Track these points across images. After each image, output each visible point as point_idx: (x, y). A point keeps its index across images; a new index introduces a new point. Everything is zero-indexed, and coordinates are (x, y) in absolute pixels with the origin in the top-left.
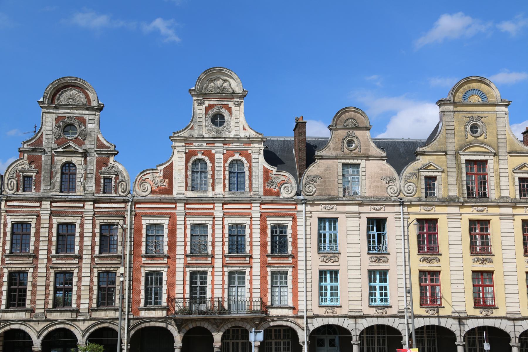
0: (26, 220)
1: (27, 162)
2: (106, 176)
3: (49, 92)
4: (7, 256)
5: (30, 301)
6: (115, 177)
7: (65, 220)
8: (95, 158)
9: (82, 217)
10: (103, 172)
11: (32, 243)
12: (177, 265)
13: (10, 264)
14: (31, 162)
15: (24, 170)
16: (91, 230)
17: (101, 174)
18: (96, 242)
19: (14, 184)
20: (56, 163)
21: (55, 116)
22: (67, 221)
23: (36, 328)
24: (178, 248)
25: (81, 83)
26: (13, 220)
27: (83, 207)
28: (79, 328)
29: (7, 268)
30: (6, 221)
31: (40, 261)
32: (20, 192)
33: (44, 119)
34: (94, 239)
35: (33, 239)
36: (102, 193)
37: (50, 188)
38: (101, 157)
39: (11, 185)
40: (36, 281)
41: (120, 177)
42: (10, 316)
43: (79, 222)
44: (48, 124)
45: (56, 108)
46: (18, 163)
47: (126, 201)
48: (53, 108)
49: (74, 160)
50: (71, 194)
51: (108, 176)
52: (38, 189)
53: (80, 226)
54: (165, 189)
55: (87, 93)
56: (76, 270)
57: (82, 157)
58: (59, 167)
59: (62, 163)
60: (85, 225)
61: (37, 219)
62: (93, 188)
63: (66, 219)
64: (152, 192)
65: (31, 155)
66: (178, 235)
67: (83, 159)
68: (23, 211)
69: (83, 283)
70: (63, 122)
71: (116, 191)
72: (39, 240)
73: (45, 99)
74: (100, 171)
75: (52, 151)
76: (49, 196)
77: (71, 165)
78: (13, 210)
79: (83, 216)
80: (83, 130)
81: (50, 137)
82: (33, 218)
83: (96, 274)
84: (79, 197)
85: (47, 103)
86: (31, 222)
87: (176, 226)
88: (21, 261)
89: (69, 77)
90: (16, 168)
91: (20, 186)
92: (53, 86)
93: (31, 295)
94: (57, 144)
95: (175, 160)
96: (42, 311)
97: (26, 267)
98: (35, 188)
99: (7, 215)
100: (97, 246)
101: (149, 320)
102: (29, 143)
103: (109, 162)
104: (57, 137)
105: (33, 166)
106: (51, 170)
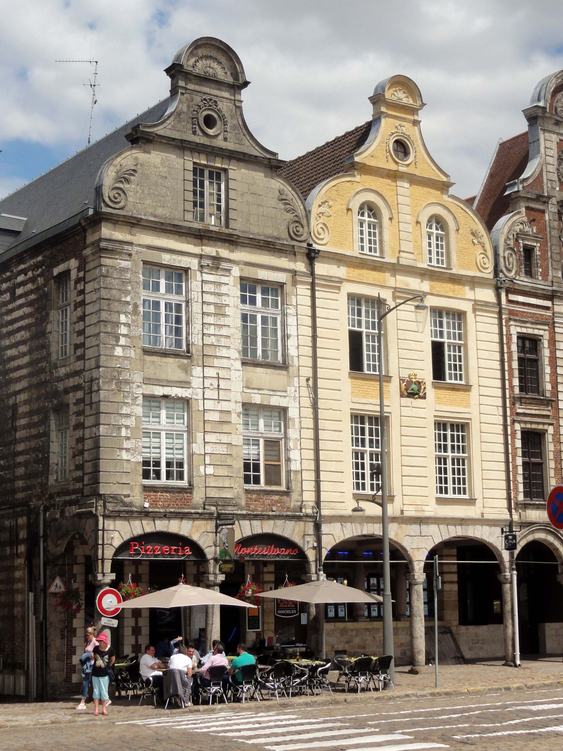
0: (536, 332)
1: (525, 219)
13: (525, 415)
26: (519, 330)
29: (519, 422)
30: (510, 331)
48: (553, 121)
52: (545, 275)
68: (530, 313)
78: (517, 311)
82: (545, 330)
86: (542, 336)
88: (536, 410)
97: (544, 424)
102: (525, 184)
105: (535, 231)
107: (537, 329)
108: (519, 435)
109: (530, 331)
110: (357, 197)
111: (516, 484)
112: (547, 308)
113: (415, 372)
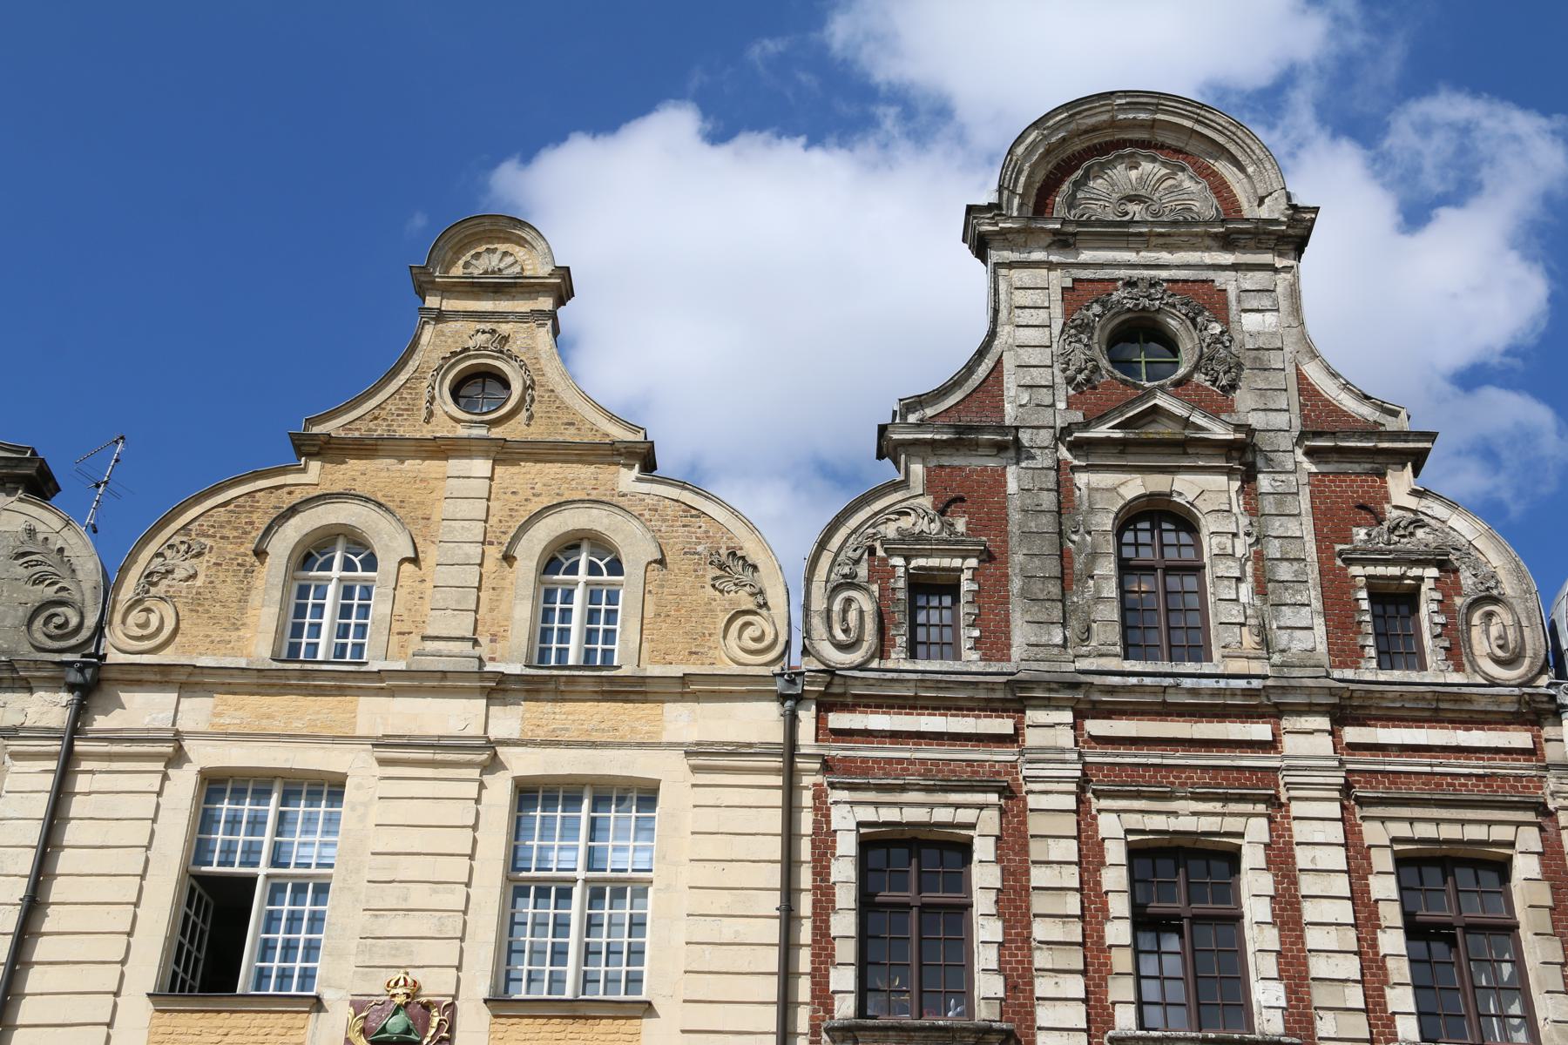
0: (942, 815)
1: (926, 502)
2: (1381, 570)
3: (1026, 167)
6: (1436, 579)
7: (1172, 819)
8: (1305, 479)
9: (1273, 801)
10: (1365, 551)
11: (985, 958)
14: (948, 505)
15: (910, 544)
17: (1349, 562)
18: (1391, 964)
19: (861, 612)
20: (1085, 507)
21: (1059, 280)
25: (1188, 123)
26: (868, 814)
30: (828, 822)
32: (897, 659)
33: (1002, 297)
34: (1374, 945)
36: (1374, 663)
37: (1065, 638)
38: (1337, 474)
39: (844, 619)
41: (1466, 579)
44: (1026, 317)
45: (1063, 241)
46: (878, 505)
48: (1048, 240)
49: (1186, 487)
50: (1189, 667)
51: (1394, 571)
53: (1269, 861)
55: (1215, 174)
57: (1230, 473)
58: (1107, 522)
59: (1121, 503)
60: (1298, 851)
61: (1003, 812)
62: (1317, 639)
63: (1175, 814)
65: (942, 467)
67: (1236, 485)
68: (923, 761)
70: (1103, 305)
72: (1027, 939)
73: (1006, 193)
74: (1338, 547)
75: (1056, 449)
76: (1069, 678)
78: (865, 760)
79: (1276, 797)
80: (1217, 340)
81: (1042, 377)
82: (981, 807)
84: (1242, 683)
85: (1015, 214)
86: (972, 826)
89: (1126, 93)
90: (871, 531)
91: (898, 625)
92: (1045, 137)
98: (977, 640)
99: (832, 786)
103: (1387, 499)
104: (1080, 378)
105: (961, 525)
106: (1061, 545)
110: (295, 521)
113: (415, 975)
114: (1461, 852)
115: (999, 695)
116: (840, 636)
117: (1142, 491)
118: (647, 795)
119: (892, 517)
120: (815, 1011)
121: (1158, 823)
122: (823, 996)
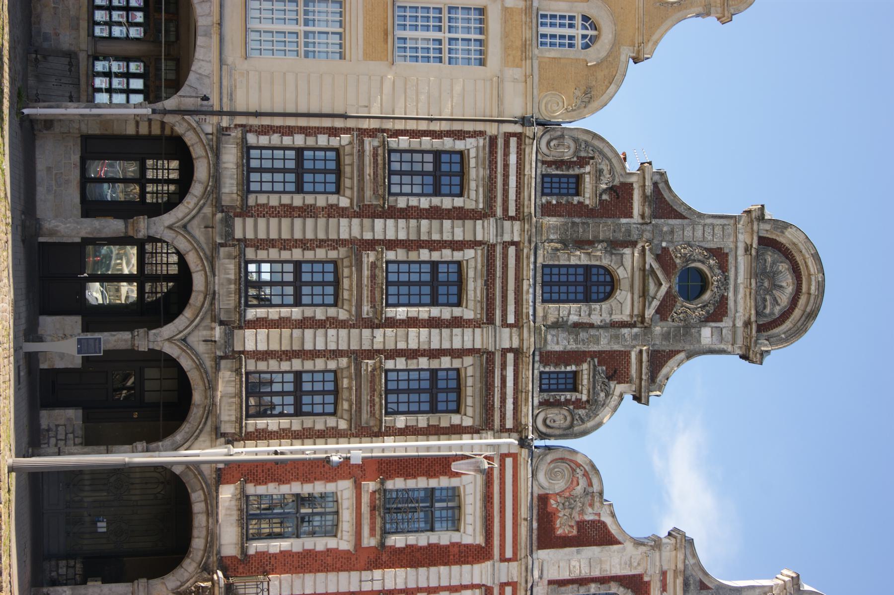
0: (473, 185)
1: (616, 183)
2: (585, 377)
4: (383, 143)
5: (264, 204)
6: (580, 400)
12: (355, 575)
16: (446, 345)
18: (415, 361)
20: (614, 252)
22: (471, 285)
23: (195, 222)
24: (401, 572)
26: (473, 153)
27: (505, 324)
28: (193, 331)
30: (469, 137)
31: (367, 222)
35: (424, 203)
40: (316, 217)
41: (582, 412)
42: (230, 156)
43: (469, 314)
47: (518, 429)
48: (749, 243)
52: (547, 210)
54: (553, 529)
56: (343, 315)
57: (631, 316)
58: (605, 262)
62: (553, 347)
64: (543, 500)
66: (433, 570)
68: (496, 177)
69: (309, 333)
71: (545, 404)
74: (596, 360)
77: (608, 289)
78: (496, 153)
82: (477, 201)
83: (332, 365)
86: (469, 198)
87: (456, 563)
93: (281, 205)
94: (660, 252)
95: (624, 549)
96: (238, 234)
100: (404, 362)
101: (212, 511)
103: (619, 383)
105: (605, 197)
107: (477, 186)
108: (334, 142)
109: (473, 173)
111: (268, 132)
112: (505, 209)
114: (463, 395)
115: (526, 210)
116: (552, 144)
117: (621, 277)
118: (482, 63)
119: (609, 167)
120: (391, 130)
121: (471, 274)
122: (397, 133)
